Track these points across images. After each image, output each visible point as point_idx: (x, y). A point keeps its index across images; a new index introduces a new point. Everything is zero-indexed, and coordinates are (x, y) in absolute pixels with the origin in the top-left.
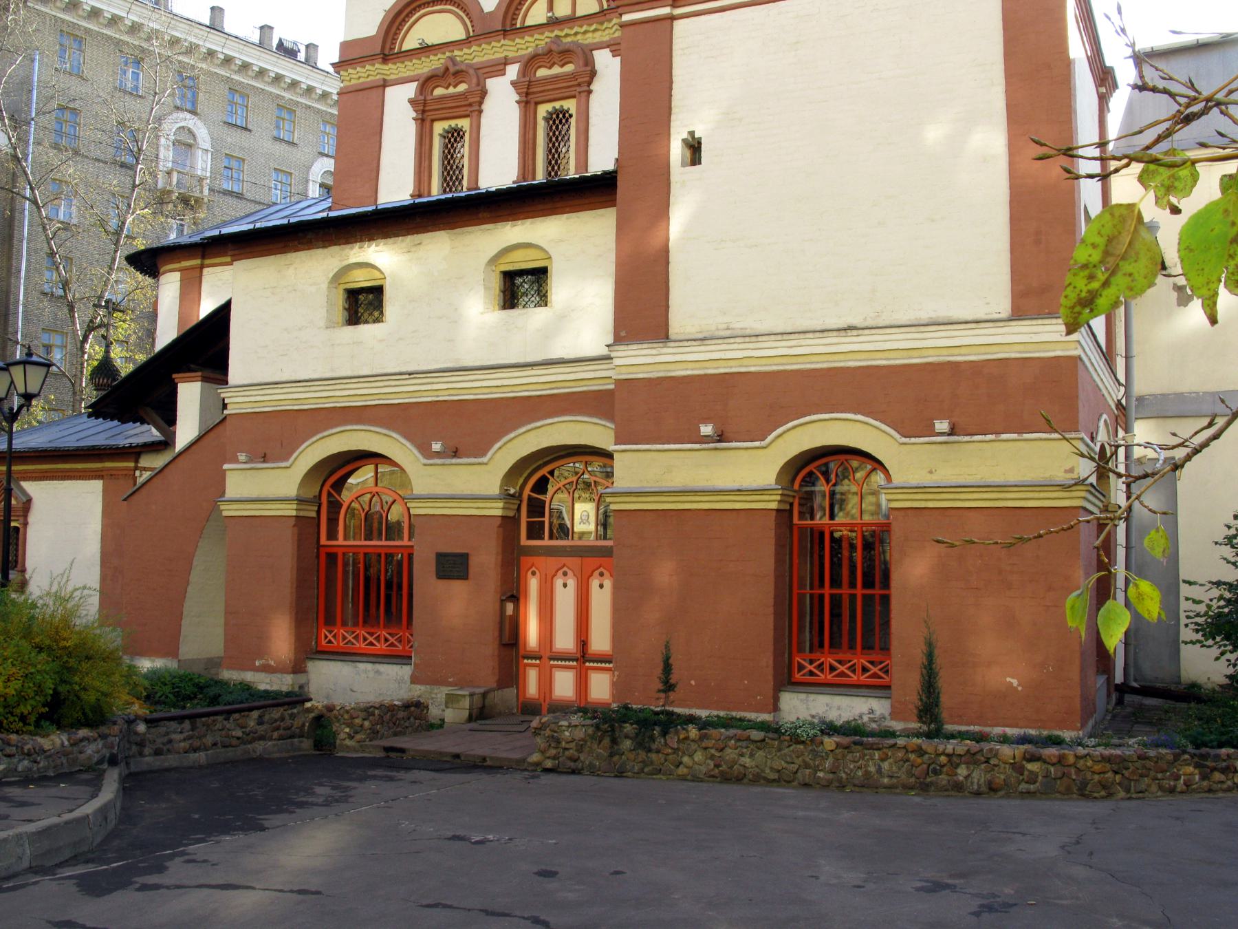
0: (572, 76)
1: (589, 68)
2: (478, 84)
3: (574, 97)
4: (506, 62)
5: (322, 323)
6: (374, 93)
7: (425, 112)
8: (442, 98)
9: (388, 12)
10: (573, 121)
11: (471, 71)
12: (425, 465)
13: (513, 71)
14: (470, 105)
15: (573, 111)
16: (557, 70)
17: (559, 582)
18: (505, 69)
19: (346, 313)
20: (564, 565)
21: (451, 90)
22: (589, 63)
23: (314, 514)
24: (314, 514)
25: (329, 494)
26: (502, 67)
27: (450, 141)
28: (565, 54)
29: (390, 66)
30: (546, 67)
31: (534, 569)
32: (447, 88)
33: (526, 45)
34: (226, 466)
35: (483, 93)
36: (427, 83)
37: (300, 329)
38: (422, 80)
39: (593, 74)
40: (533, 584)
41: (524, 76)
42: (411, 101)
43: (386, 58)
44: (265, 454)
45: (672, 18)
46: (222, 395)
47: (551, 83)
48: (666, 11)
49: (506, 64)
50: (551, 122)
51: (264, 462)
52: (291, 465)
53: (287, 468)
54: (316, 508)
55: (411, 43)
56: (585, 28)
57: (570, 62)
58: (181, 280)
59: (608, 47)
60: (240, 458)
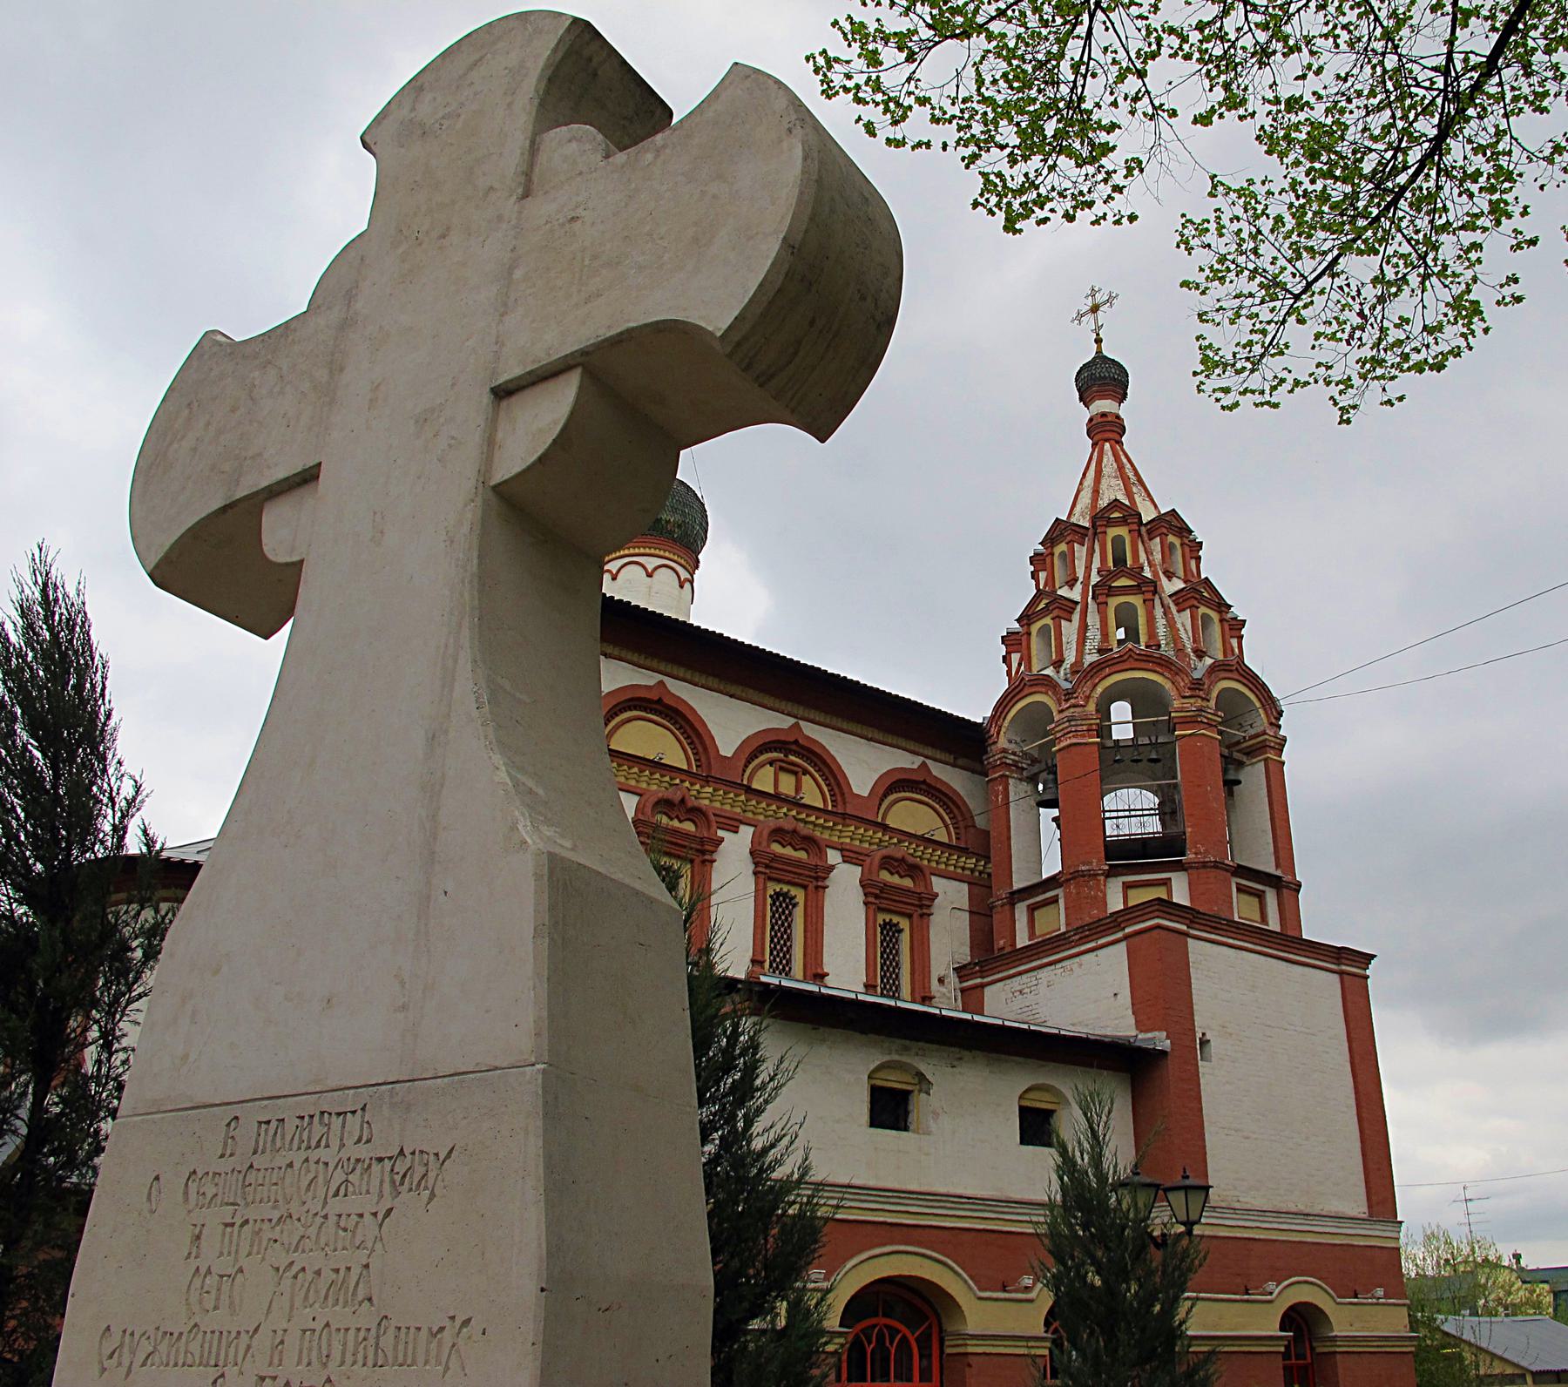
12: (980, 1298)
13: (747, 832)
21: (676, 823)
56: (821, 821)
59: (841, 850)
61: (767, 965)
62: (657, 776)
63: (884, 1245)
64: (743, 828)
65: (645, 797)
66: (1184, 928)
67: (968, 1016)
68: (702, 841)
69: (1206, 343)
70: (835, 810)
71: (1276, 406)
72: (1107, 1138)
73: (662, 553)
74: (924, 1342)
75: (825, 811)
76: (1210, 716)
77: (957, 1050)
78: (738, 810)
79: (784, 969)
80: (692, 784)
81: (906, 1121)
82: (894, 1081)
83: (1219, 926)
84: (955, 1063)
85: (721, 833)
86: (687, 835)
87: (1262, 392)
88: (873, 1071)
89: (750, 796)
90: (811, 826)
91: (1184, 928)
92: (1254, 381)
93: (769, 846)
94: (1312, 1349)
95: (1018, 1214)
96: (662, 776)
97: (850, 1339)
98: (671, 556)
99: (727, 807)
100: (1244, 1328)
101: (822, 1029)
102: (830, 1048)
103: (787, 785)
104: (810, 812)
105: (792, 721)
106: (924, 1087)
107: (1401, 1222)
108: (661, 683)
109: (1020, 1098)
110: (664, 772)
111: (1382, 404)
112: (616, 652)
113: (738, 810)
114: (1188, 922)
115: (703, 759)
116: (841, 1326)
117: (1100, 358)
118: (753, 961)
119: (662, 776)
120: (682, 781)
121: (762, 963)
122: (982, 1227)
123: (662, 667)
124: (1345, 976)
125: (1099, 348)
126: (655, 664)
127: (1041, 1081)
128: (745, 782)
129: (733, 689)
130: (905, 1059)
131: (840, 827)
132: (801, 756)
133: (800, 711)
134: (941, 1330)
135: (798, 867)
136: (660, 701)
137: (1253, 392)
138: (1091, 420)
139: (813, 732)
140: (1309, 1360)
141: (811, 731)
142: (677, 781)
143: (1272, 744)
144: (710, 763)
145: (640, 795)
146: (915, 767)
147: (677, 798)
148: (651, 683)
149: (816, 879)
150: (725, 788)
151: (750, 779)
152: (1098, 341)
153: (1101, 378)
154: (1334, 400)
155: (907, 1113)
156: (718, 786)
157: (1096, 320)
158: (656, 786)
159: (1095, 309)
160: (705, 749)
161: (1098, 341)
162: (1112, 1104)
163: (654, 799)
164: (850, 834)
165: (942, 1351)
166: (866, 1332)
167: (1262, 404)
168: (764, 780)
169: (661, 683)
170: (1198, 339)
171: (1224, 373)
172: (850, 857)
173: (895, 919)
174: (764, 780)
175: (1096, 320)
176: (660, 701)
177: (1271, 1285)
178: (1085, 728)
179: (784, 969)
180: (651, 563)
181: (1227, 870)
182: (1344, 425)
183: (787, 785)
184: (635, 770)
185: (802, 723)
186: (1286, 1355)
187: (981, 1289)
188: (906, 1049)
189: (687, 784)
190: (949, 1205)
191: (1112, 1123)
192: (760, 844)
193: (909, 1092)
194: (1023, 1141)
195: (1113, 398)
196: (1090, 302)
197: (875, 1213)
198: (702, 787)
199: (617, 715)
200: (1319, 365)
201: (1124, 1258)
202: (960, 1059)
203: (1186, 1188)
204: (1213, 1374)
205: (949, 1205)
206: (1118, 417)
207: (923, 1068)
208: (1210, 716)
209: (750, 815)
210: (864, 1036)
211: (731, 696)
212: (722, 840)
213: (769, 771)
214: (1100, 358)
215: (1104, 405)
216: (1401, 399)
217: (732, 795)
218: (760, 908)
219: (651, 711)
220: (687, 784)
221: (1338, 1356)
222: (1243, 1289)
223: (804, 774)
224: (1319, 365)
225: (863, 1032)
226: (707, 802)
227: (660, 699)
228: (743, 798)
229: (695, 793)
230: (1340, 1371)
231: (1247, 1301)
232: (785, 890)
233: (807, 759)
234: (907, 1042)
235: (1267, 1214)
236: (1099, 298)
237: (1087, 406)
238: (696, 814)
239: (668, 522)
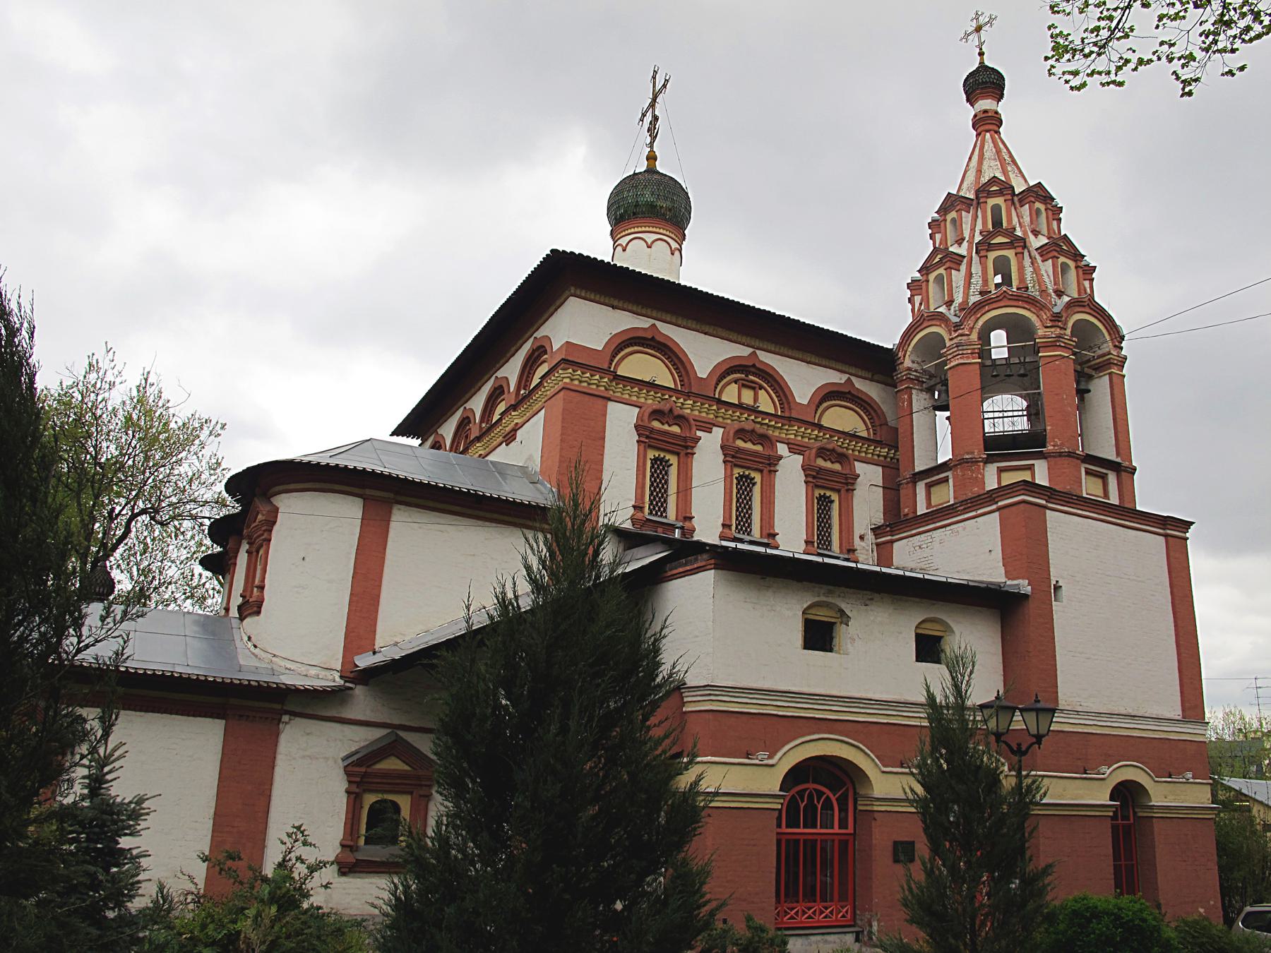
12: (884, 772)
13: (718, 432)
16: (749, 446)
21: (666, 427)
37: (780, 646)
52: (777, 763)
53: (772, 766)
56: (773, 423)
59: (788, 444)
61: (734, 528)
62: (652, 393)
63: (814, 733)
64: (715, 429)
65: (643, 409)
66: (1044, 502)
67: (878, 569)
68: (685, 439)
69: (1057, 31)
70: (783, 415)
71: (1120, 84)
72: (968, 693)
73: (658, 230)
74: (843, 802)
75: (775, 416)
76: (1066, 341)
77: (869, 593)
78: (712, 416)
79: (746, 530)
80: (678, 398)
81: (831, 645)
82: (822, 615)
83: (1071, 501)
84: (868, 602)
85: (699, 433)
86: (674, 435)
87: (1108, 73)
88: (805, 610)
89: (720, 406)
90: (765, 427)
92: (1101, 64)
93: (734, 442)
94: (1135, 813)
96: (656, 393)
97: (788, 799)
98: (665, 232)
99: (704, 415)
100: (1082, 798)
101: (768, 579)
102: (774, 592)
103: (748, 397)
104: (764, 416)
105: (751, 350)
106: (844, 620)
107: (1208, 723)
108: (654, 325)
109: (916, 627)
110: (658, 390)
111: (1223, 75)
112: (620, 305)
113: (712, 416)
114: (1046, 498)
115: (686, 380)
116: (781, 790)
117: (983, 68)
118: (723, 525)
119: (656, 393)
120: (670, 396)
121: (729, 526)
122: (885, 721)
123: (654, 314)
124: (1169, 538)
125: (982, 59)
126: (649, 312)
127: (932, 615)
128: (717, 396)
129: (707, 329)
130: (830, 600)
131: (787, 427)
132: (755, 375)
133: (757, 343)
134: (855, 793)
135: (756, 457)
137: (1100, 73)
138: (975, 116)
140: (1132, 821)
141: (766, 358)
142: (667, 397)
143: (1115, 362)
144: (690, 383)
145: (640, 407)
146: (843, 382)
147: (666, 408)
148: (646, 326)
149: (770, 464)
150: (701, 400)
151: (720, 393)
152: (981, 54)
153: (983, 82)
154: (1177, 75)
155: (832, 639)
156: (696, 399)
157: (980, 38)
158: (651, 402)
159: (978, 29)
160: (687, 372)
161: (981, 54)
162: (973, 666)
163: (650, 410)
164: (793, 433)
165: (855, 808)
166: (801, 793)
167: (1108, 84)
168: (730, 394)
169: (654, 325)
170: (1049, 28)
171: (1073, 58)
172: (794, 448)
173: (828, 493)
174: (730, 394)
175: (980, 38)
177: (1104, 769)
178: (969, 351)
179: (746, 530)
180: (650, 238)
181: (1078, 459)
182: (1186, 98)
183: (748, 397)
184: (636, 389)
185: (758, 352)
186: (1114, 818)
187: (885, 766)
188: (830, 592)
189: (674, 398)
190: (861, 705)
191: (972, 682)
192: (728, 440)
193: (835, 623)
194: (917, 661)
195: (993, 98)
196: (974, 24)
198: (685, 400)
199: (622, 350)
200: (1162, 43)
201: (979, 792)
202: (872, 599)
203: (1038, 711)
204: (1049, 884)
205: (861, 705)
206: (996, 113)
207: (843, 606)
208: (1066, 341)
209: (721, 420)
211: (706, 334)
212: (699, 438)
213: (734, 387)
214: (983, 68)
215: (986, 104)
216: (1242, 69)
217: (707, 406)
218: (728, 486)
220: (674, 398)
221: (1154, 820)
222: (1082, 770)
223: (760, 389)
224: (1162, 43)
225: (799, 580)
226: (689, 411)
227: (653, 337)
228: (715, 407)
229: (680, 405)
230: (1156, 830)
231: (1085, 778)
232: (747, 473)
233: (762, 378)
234: (831, 588)
236: (982, 20)
237: (972, 105)
238: (680, 420)
239: (662, 207)
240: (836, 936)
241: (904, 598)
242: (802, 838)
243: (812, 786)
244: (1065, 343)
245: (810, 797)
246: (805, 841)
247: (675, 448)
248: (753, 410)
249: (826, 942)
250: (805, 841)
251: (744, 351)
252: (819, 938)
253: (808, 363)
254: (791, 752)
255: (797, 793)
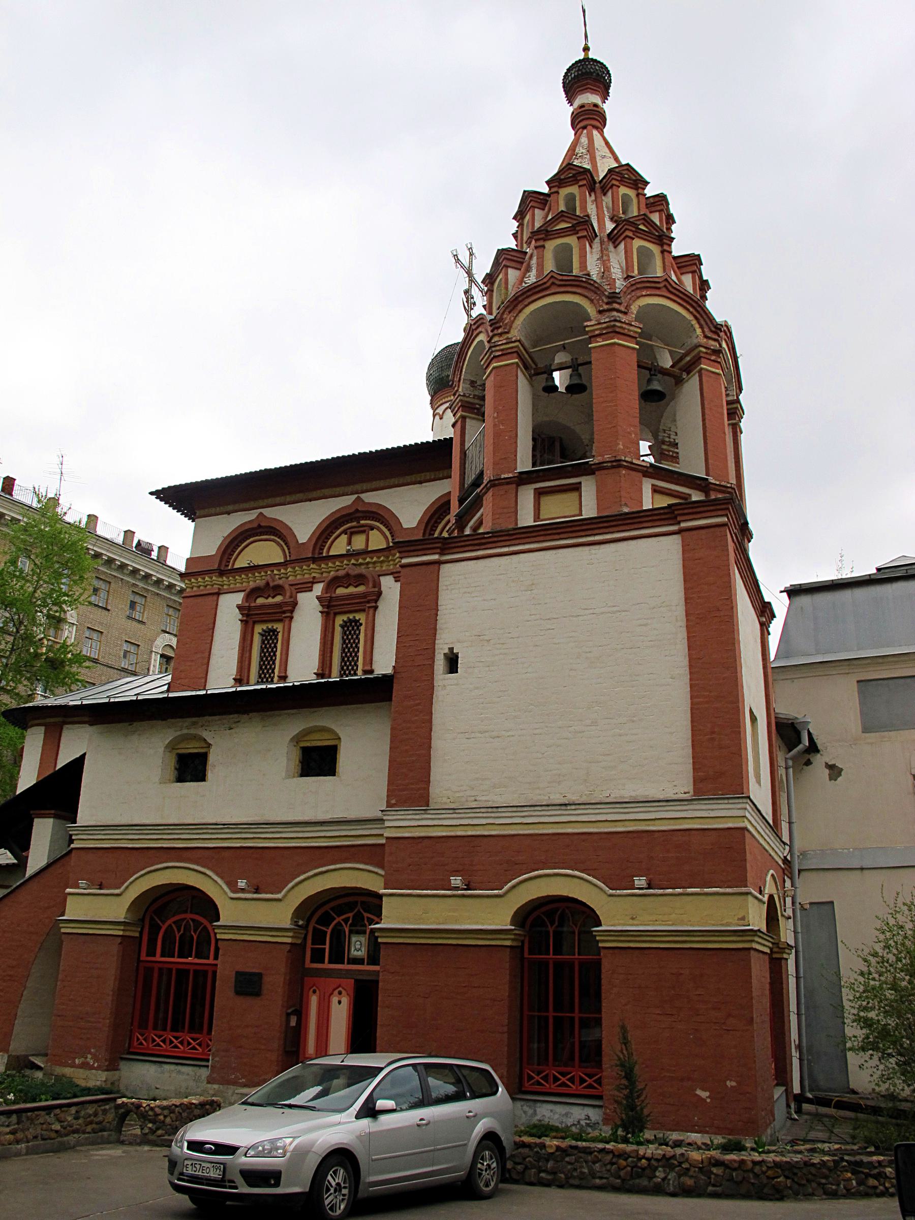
0: (364, 595)
1: (376, 589)
2: (291, 597)
3: (364, 610)
4: (314, 582)
5: (157, 779)
6: (210, 598)
7: (249, 616)
8: (262, 606)
9: (225, 538)
10: (362, 628)
11: (287, 587)
13: (318, 589)
14: (284, 612)
15: (363, 621)
17: (335, 1000)
18: (312, 587)
19: (176, 772)
20: (339, 986)
21: (270, 600)
22: (377, 585)
23: (137, 935)
24: (137, 935)
25: (152, 919)
26: (310, 585)
27: (266, 639)
28: (360, 579)
29: (225, 578)
30: (344, 587)
31: (314, 988)
32: (267, 598)
33: (331, 570)
34: (68, 890)
35: (295, 604)
36: (253, 593)
38: (248, 590)
39: (380, 594)
40: (314, 1000)
41: (327, 593)
42: (239, 607)
43: (221, 573)
44: (101, 883)
45: (439, 563)
46: (71, 833)
47: (347, 599)
48: (436, 557)
49: (313, 583)
50: (346, 629)
51: (100, 889)
54: (139, 929)
55: (241, 563)
56: (375, 559)
57: (363, 584)
58: (45, 733)
59: (392, 574)
60: (80, 885)
66: (436, 557)
76: (502, 347)
77: (236, 715)
82: (192, 748)
83: (483, 541)
90: (379, 565)
91: (436, 557)
95: (169, 834)
96: (260, 573)
100: (456, 921)
101: (135, 724)
103: (359, 542)
108: (261, 513)
110: (260, 570)
114: (438, 551)
122: (238, 845)
127: (311, 724)
130: (193, 731)
136: (260, 526)
139: (370, 498)
141: (370, 498)
143: (597, 332)
148: (349, 503)
150: (298, 564)
176: (260, 526)
181: (508, 483)
183: (359, 542)
188: (194, 723)
197: (119, 842)
208: (502, 347)
210: (164, 722)
211: (310, 500)
219: (261, 534)
223: (372, 529)
234: (194, 719)
235: (500, 810)
240: (190, 1068)
241: (277, 712)
242: (174, 967)
243: (189, 916)
244: (502, 350)
245: (187, 928)
246: (160, 969)
247: (277, 617)
248: (365, 552)
249: (179, 1072)
250: (196, 971)
251: (346, 501)
252: (173, 1067)
253: (420, 483)
254: (138, 881)
255: (174, 923)
